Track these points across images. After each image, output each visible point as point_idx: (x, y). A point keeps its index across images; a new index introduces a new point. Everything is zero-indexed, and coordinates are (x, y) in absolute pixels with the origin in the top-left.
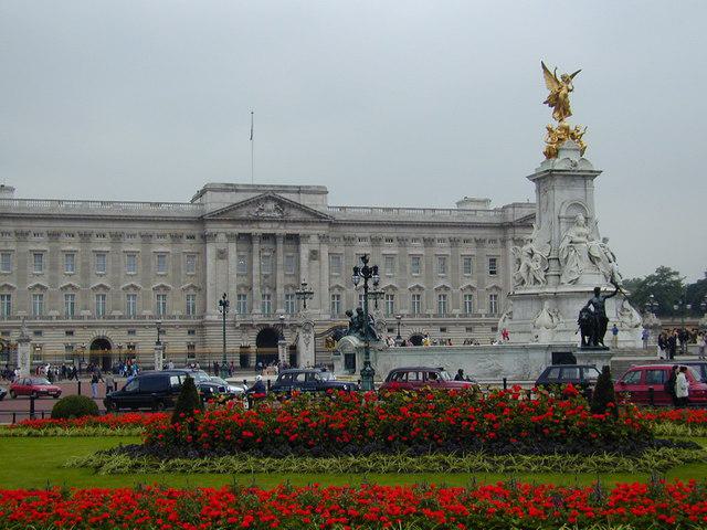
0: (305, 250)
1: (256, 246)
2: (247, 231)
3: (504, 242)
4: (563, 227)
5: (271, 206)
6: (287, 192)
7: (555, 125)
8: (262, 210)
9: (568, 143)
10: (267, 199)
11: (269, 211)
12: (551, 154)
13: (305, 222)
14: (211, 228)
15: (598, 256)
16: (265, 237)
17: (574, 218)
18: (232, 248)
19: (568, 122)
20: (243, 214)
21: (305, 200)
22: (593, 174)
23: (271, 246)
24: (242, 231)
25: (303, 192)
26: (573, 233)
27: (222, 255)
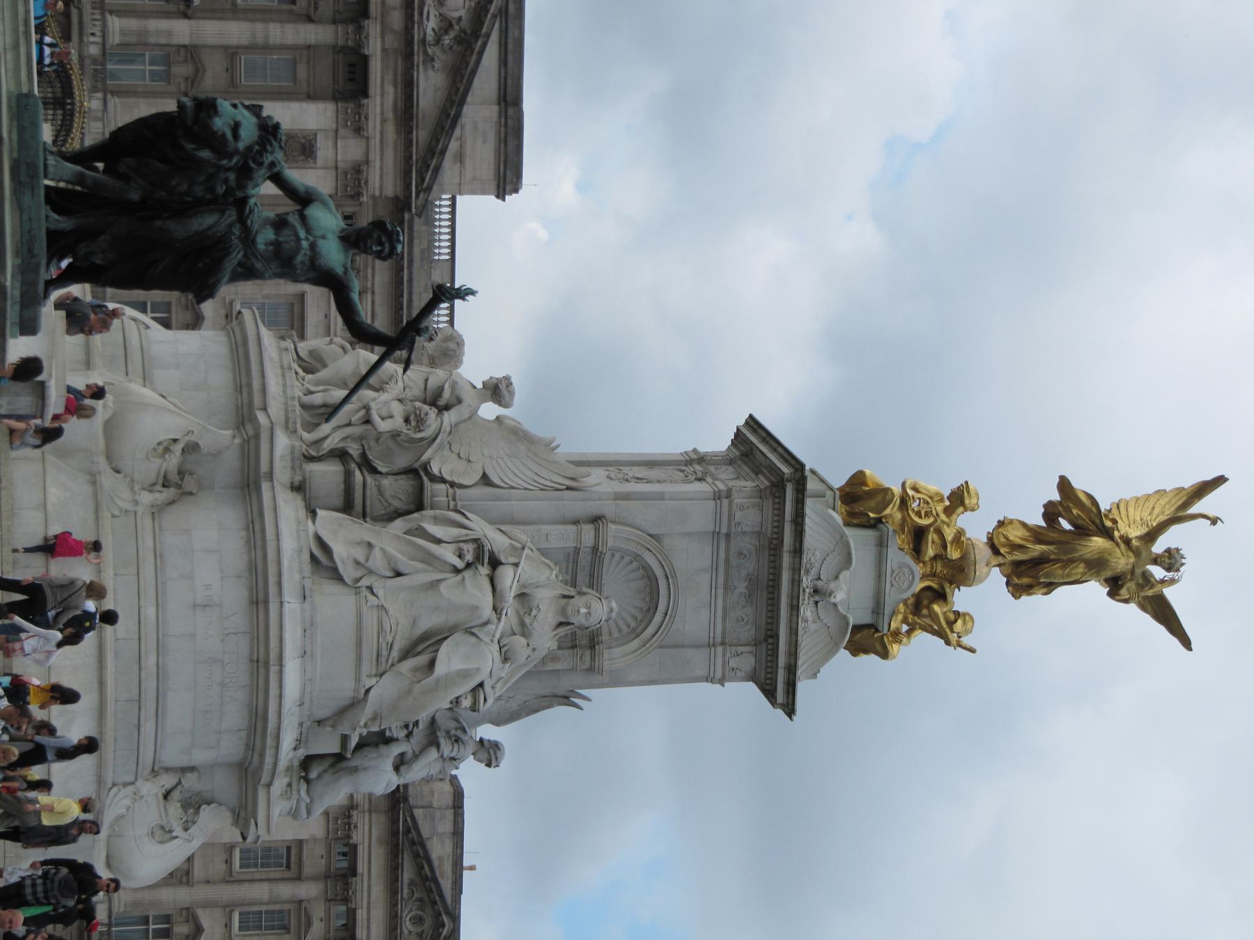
4: (561, 537)
6: (503, 62)
7: (975, 526)
9: (909, 577)
12: (860, 499)
13: (406, 114)
15: (441, 669)
17: (595, 582)
19: (995, 580)
21: (479, 112)
22: (779, 687)
25: (503, 113)
26: (533, 573)
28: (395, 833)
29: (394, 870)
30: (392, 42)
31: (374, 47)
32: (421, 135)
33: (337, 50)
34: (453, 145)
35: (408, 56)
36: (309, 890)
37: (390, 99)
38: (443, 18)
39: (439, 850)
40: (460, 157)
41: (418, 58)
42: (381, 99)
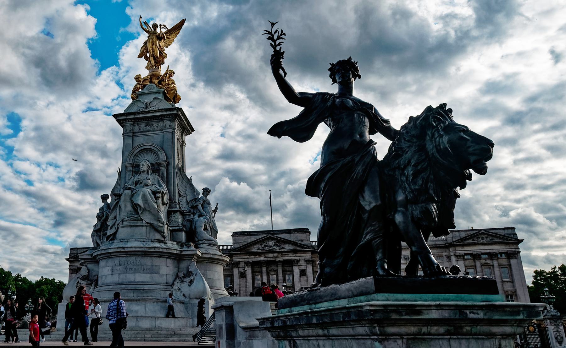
0: (296, 270)
1: (264, 269)
2: (258, 259)
3: (449, 257)
5: (271, 243)
8: (265, 246)
10: (269, 239)
11: (271, 246)
13: (295, 252)
14: (236, 259)
16: (269, 263)
18: (249, 271)
20: (254, 249)
23: (275, 268)
24: (254, 260)
27: (243, 275)
28: (460, 245)
29: (469, 245)
30: (280, 255)
31: (281, 259)
32: (298, 249)
33: (283, 266)
34: (300, 242)
35: (282, 252)
36: (478, 264)
37: (291, 255)
38: (274, 245)
39: (463, 235)
40: (302, 241)
41: (282, 250)
42: (291, 257)
